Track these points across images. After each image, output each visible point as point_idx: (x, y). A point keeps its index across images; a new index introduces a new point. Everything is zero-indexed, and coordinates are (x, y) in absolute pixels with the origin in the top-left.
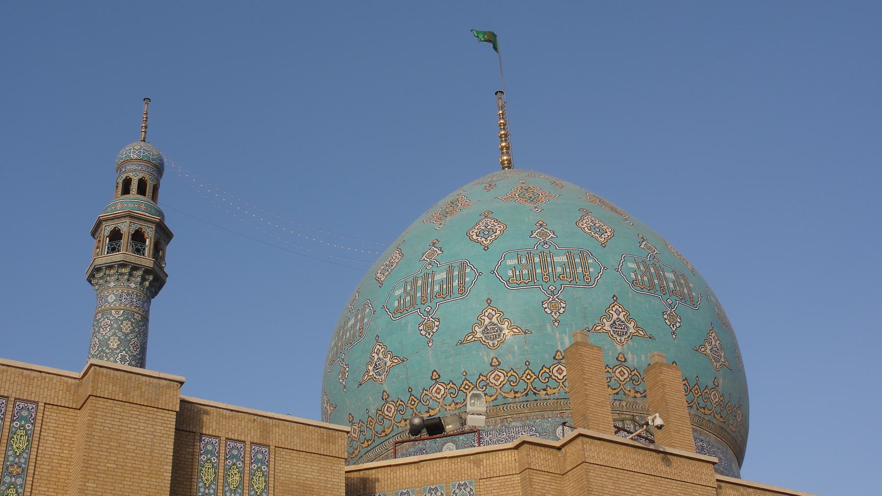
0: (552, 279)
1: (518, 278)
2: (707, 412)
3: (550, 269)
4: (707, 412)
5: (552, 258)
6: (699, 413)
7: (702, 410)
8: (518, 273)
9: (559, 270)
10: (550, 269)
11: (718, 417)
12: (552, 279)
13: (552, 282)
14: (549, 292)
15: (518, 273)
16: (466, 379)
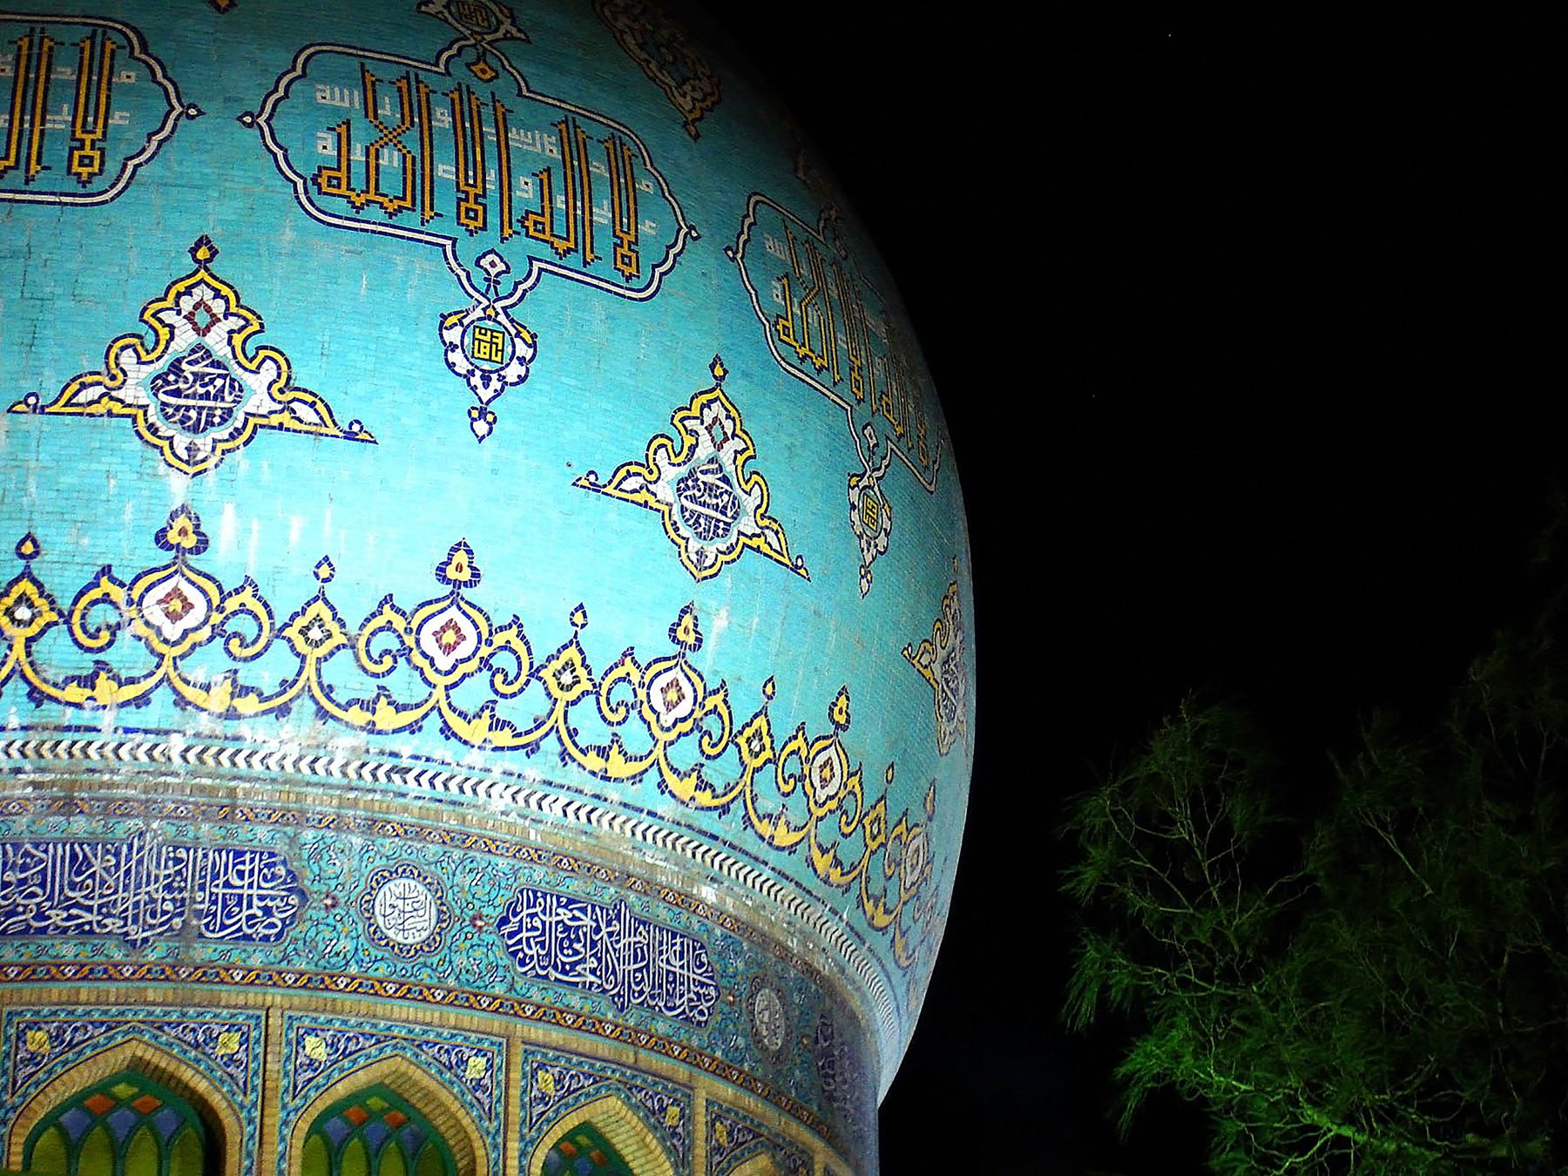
0: (493, 220)
1: (358, 183)
2: (617, 766)
3: (492, 175)
4: (617, 766)
5: (502, 126)
6: (572, 775)
7: (593, 762)
8: (358, 155)
9: (526, 192)
10: (492, 175)
11: (685, 788)
12: (493, 220)
13: (491, 238)
14: (478, 278)
15: (358, 155)
16: (321, 597)
